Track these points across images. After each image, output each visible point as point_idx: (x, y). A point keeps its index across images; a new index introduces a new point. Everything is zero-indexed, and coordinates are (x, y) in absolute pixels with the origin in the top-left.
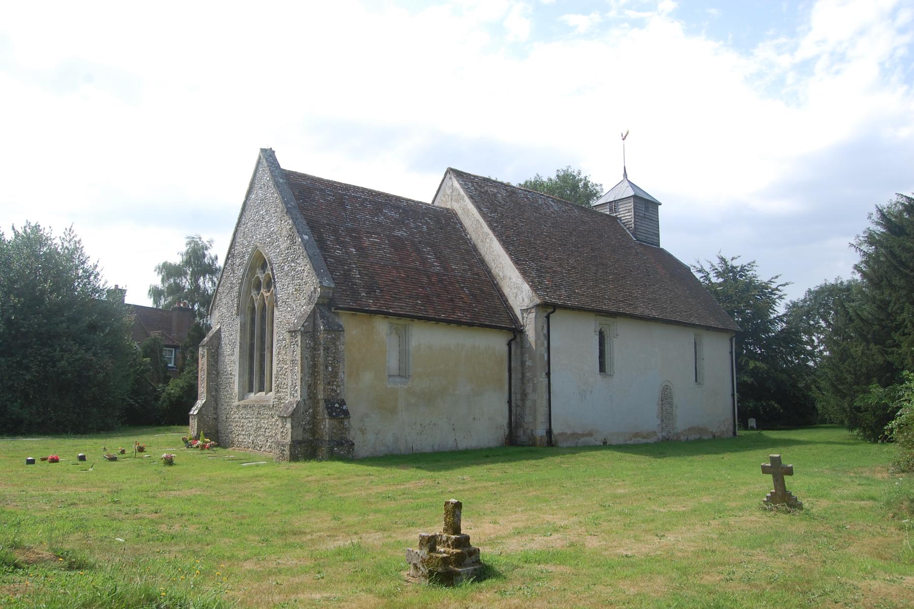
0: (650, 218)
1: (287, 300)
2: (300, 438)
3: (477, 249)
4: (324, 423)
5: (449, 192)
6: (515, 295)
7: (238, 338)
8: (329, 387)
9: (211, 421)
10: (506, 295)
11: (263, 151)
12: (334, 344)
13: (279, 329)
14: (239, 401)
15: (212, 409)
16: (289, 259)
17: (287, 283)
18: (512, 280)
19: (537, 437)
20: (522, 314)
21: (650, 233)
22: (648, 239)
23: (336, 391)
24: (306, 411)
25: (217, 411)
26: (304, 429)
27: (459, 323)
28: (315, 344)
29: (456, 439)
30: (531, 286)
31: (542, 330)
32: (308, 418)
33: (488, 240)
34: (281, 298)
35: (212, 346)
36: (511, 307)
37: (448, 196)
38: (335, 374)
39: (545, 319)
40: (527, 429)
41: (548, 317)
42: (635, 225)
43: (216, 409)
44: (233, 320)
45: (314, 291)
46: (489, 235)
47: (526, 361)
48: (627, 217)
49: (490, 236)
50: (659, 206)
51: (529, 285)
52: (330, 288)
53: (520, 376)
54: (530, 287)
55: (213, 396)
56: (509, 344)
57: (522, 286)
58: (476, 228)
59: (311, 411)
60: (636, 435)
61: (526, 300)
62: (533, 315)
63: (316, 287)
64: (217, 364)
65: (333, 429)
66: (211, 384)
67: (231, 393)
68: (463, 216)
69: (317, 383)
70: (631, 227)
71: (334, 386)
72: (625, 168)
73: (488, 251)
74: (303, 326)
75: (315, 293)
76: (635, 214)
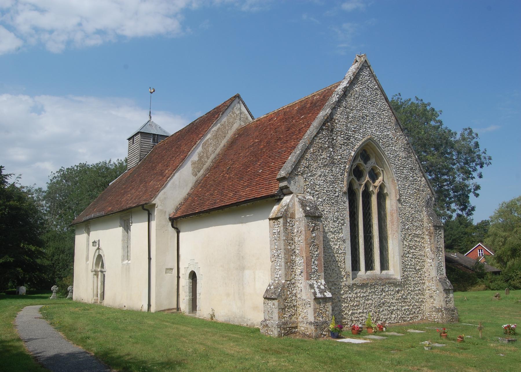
5: (238, 112)
14: (353, 279)
37: (237, 115)
44: (338, 196)
72: (150, 112)
75: (431, 201)
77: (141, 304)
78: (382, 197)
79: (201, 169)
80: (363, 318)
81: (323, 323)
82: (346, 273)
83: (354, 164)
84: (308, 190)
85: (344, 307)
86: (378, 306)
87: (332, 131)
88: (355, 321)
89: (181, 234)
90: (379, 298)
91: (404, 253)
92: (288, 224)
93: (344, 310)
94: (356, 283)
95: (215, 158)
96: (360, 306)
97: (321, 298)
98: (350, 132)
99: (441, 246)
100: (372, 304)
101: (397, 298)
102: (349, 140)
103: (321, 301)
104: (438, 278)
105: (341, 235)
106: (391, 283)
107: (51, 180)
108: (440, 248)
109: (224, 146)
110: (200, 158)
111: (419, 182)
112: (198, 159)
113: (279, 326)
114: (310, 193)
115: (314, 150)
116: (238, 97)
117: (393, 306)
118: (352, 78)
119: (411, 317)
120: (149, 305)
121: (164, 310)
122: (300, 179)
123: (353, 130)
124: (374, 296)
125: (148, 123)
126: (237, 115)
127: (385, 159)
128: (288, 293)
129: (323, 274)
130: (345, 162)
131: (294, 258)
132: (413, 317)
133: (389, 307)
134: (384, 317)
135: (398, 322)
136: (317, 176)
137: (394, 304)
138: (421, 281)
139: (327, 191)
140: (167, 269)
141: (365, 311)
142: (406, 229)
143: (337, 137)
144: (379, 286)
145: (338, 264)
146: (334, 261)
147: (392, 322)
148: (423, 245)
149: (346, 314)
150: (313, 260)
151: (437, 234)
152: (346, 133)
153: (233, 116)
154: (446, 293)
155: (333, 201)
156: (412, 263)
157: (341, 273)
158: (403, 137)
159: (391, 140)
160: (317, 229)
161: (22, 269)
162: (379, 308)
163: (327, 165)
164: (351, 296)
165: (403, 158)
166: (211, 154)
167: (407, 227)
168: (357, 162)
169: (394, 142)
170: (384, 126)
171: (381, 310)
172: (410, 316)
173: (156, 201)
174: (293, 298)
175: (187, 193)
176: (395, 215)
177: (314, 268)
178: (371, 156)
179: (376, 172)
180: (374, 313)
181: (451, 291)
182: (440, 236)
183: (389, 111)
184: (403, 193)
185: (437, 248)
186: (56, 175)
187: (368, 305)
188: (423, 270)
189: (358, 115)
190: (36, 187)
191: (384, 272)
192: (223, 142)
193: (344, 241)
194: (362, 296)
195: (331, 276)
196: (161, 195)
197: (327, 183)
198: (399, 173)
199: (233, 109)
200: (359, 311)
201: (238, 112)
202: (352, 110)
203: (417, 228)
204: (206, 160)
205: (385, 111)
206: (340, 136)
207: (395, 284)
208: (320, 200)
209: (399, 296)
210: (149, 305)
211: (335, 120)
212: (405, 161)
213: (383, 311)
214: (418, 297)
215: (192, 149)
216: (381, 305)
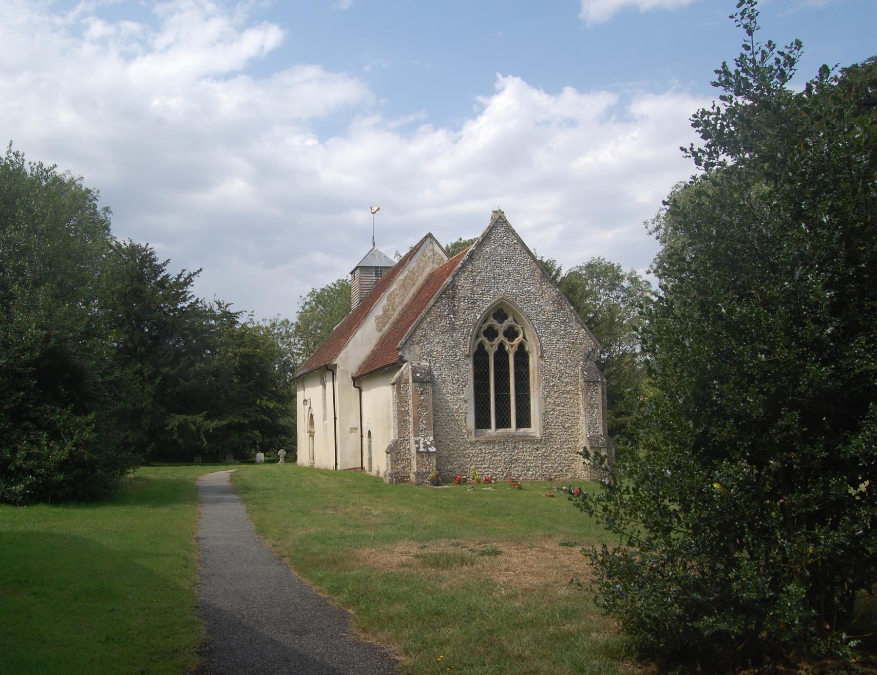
5: (430, 254)
37: (429, 258)
44: (459, 360)
75: (594, 353)
77: (332, 465)
78: (522, 355)
79: (386, 323)
80: (490, 473)
81: (425, 473)
82: (468, 430)
84: (424, 357)
87: (453, 298)
88: (479, 475)
89: (363, 393)
90: (510, 455)
91: (546, 412)
92: (402, 389)
94: (480, 440)
95: (403, 310)
96: (486, 461)
97: (424, 452)
98: (476, 296)
100: (501, 460)
102: (475, 303)
103: (424, 454)
104: (588, 436)
105: (462, 396)
107: (303, 308)
109: (414, 295)
110: (385, 311)
112: (382, 313)
113: (391, 475)
114: (426, 360)
116: (430, 236)
118: (480, 240)
119: (556, 475)
120: (336, 464)
121: (350, 469)
122: (417, 349)
123: (481, 294)
124: (503, 453)
125: (371, 253)
126: (429, 258)
127: (523, 317)
128: (402, 448)
129: (432, 431)
130: (469, 326)
131: (408, 418)
133: (525, 464)
135: (537, 479)
136: (434, 343)
137: (532, 462)
138: (573, 439)
139: (445, 356)
140: (351, 429)
141: (491, 466)
148: (576, 401)
150: (421, 420)
153: (424, 259)
155: (453, 365)
159: (534, 295)
160: (426, 393)
161: (259, 432)
164: (473, 452)
166: (398, 306)
167: (551, 384)
168: (489, 323)
171: (513, 466)
173: (337, 361)
174: (407, 452)
175: (371, 350)
176: (536, 373)
178: (509, 315)
179: (516, 330)
181: (602, 450)
183: (533, 264)
186: (308, 300)
187: (495, 461)
188: (576, 428)
189: (488, 277)
190: (282, 318)
191: (522, 430)
192: (412, 290)
193: (465, 401)
194: (487, 452)
196: (342, 354)
197: (447, 348)
200: (484, 466)
201: (431, 253)
202: (479, 273)
204: (392, 313)
205: (527, 265)
206: (464, 302)
207: (532, 440)
208: (438, 365)
209: (539, 454)
210: (336, 464)
211: (457, 286)
213: (515, 467)
214: (567, 456)
215: (375, 303)
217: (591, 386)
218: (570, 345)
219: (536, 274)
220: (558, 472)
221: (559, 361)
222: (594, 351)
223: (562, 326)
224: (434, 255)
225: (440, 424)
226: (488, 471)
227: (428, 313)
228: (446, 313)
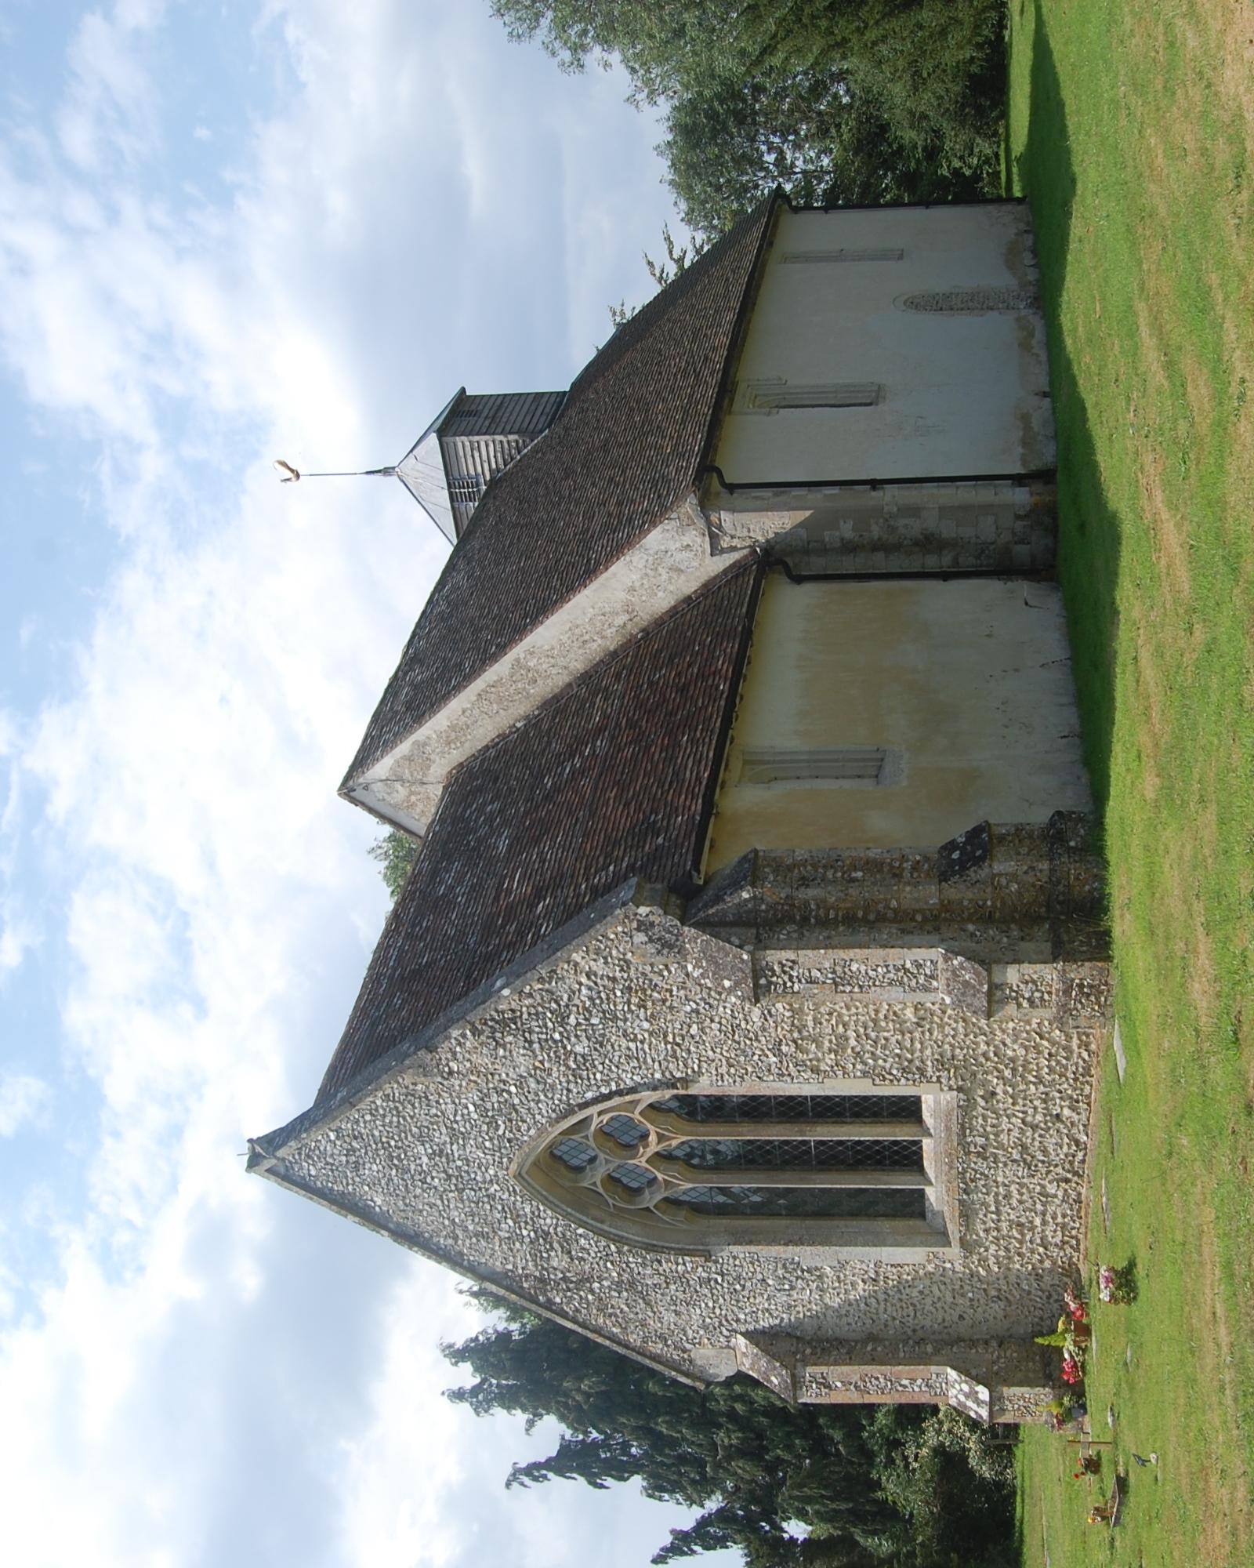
0: (495, 408)
1: (670, 1038)
2: (1047, 947)
3: (553, 697)
4: (1004, 881)
5: (401, 791)
6: (674, 575)
7: (775, 1250)
8: (907, 874)
9: (1008, 1354)
10: (673, 603)
11: (254, 1162)
12: (790, 868)
13: (750, 1069)
14: (948, 1244)
15: (974, 1351)
16: (557, 1036)
17: (624, 1043)
18: (637, 584)
19: (1033, 500)
20: (723, 551)
21: (533, 407)
22: (547, 410)
23: (918, 862)
24: (973, 935)
25: (978, 1340)
26: (1022, 939)
27: (740, 663)
28: (792, 920)
29: (1042, 666)
30: (654, 524)
31: (764, 499)
32: (991, 932)
33: (531, 664)
34: (664, 1064)
35: (795, 1354)
36: (705, 585)
37: (411, 793)
38: (873, 866)
39: (735, 495)
40: (1014, 534)
41: (732, 488)
42: (510, 433)
43: (973, 1343)
44: (722, 1275)
45: (646, 931)
46: (518, 660)
47: (842, 539)
48: (492, 454)
49: (522, 656)
50: (468, 393)
51: (649, 531)
52: (639, 886)
53: (879, 556)
54: (655, 526)
55: (937, 1351)
56: (799, 580)
57: (651, 552)
58: (500, 700)
59: (971, 927)
60: (1025, 346)
61: (686, 540)
62: (726, 518)
63: (635, 925)
64: (847, 1341)
65: (1019, 854)
66: (902, 1355)
67: (927, 1282)
68: (467, 745)
69: (894, 910)
70: (517, 442)
71: (905, 865)
72: (368, 473)
73: (561, 662)
74: (741, 947)
75: (652, 924)
76: (485, 434)
83: (611, 1201)
85: (1022, 1266)
86: (1029, 1168)
90: (1005, 1165)
93: (1030, 1267)
96: (1023, 1220)
99: (827, 965)
101: (1010, 1101)
106: (963, 1128)
108: (834, 972)
111: (596, 983)
115: (614, 1326)
117: (1034, 1116)
126: (411, 793)
132: (1079, 1039)
134: (1065, 1148)
141: (1039, 1207)
142: (781, 1062)
143: (555, 1269)
144: (969, 1165)
145: (907, 1281)
146: (899, 1291)
147: (1085, 1119)
149: (1041, 1262)
151: (785, 983)
152: (531, 1242)
154: (1004, 1001)
156: (893, 1040)
157: (930, 1273)
158: (458, 1049)
159: (487, 1095)
160: (824, 1378)
162: (1036, 1166)
163: (643, 1299)
165: (533, 1052)
169: (491, 1085)
170: (451, 1117)
172: (1075, 1047)
177: (920, 1387)
180: (1050, 1177)
181: (997, 980)
182: (792, 968)
184: (656, 1065)
185: (836, 984)
193: (843, 1265)
195: (939, 1298)
198: (592, 1076)
199: (395, 806)
203: (769, 1012)
205: (396, 1108)
209: (1005, 1093)
212: (542, 1048)
216: (1029, 1159)
217: (771, 983)
218: (635, 1000)
219: (419, 1087)
220: (1069, 1038)
221: (692, 1037)
222: (644, 926)
223: (572, 1020)
224: (400, 779)
225: (910, 1319)
226: (1055, 1213)
227: (597, 1331)
228: (590, 1297)
